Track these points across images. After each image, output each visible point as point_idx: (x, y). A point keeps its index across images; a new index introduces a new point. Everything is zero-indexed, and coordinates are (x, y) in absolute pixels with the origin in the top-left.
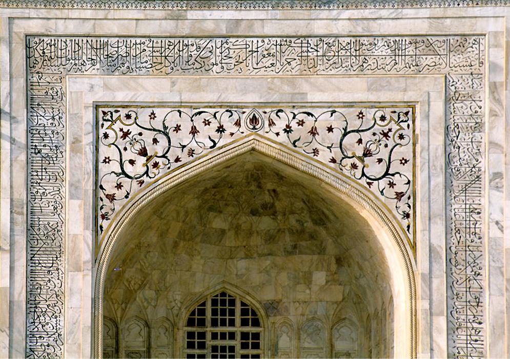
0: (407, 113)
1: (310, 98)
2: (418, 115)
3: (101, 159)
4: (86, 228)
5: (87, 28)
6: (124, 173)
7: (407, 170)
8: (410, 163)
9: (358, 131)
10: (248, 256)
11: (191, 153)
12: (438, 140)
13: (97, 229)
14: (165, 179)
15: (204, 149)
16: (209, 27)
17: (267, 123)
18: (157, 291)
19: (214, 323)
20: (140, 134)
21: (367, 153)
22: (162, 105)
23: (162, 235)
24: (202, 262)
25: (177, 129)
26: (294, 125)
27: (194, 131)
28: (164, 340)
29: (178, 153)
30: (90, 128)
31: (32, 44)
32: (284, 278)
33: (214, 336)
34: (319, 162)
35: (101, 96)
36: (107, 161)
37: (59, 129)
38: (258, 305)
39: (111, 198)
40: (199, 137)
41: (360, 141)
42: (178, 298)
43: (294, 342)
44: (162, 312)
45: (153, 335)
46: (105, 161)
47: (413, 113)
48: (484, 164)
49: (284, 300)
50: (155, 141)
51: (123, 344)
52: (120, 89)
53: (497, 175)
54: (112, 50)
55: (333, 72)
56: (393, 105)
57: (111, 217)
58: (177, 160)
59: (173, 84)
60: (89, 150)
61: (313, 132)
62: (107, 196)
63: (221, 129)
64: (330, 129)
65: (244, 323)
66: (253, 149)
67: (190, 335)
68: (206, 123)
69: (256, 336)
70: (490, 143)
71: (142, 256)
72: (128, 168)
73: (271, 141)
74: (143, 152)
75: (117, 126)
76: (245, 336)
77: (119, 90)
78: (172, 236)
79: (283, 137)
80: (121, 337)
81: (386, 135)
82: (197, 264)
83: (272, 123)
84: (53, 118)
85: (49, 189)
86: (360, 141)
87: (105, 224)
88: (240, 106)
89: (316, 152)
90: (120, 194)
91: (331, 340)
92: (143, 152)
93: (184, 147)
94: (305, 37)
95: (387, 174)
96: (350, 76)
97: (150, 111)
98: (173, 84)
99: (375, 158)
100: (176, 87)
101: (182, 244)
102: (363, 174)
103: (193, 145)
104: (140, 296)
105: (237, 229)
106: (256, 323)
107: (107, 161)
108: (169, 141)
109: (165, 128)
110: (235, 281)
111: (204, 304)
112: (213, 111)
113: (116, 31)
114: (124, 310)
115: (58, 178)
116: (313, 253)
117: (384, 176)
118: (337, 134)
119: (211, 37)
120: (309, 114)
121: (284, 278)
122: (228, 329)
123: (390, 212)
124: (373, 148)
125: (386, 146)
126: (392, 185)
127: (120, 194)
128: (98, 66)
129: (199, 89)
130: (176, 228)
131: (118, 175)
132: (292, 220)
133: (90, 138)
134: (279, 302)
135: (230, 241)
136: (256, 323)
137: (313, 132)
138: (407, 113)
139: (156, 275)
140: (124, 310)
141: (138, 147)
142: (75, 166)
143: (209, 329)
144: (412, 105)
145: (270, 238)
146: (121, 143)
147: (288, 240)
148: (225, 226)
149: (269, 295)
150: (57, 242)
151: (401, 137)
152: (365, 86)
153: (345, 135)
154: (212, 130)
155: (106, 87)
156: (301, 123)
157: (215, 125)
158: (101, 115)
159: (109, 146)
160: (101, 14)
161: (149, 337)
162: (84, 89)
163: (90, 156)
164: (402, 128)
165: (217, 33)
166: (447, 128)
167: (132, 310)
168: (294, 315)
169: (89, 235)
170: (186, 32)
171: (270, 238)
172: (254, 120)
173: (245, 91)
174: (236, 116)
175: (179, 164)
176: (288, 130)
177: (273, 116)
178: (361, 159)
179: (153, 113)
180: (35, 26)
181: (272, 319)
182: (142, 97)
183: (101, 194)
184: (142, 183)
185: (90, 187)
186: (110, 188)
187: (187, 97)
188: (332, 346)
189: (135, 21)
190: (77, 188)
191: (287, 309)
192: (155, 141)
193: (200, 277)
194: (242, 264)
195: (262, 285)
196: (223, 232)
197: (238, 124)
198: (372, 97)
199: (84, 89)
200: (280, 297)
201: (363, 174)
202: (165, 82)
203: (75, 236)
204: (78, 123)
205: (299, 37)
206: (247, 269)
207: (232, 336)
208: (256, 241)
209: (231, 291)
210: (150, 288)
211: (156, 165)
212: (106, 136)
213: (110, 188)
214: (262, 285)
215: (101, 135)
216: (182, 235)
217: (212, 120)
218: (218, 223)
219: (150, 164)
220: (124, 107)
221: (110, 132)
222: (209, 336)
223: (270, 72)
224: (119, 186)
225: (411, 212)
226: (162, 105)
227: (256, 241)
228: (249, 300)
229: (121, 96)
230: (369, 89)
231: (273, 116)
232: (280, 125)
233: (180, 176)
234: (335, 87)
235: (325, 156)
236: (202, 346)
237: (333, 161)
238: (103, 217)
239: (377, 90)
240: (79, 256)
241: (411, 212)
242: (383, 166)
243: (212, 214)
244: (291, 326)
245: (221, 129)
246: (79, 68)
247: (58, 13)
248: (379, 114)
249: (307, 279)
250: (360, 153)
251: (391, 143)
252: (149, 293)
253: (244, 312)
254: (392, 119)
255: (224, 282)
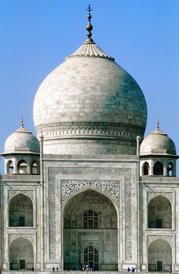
0: (118, 182)
1: (100, 179)
2: (120, 183)
3: (62, 190)
4: (60, 203)
5: (59, 166)
6: (66, 193)
7: (118, 193)
8: (119, 191)
9: (109, 185)
10: (95, 203)
11: (79, 189)
12: (124, 187)
13: (61, 203)
14: (74, 194)
15: (82, 188)
16: (82, 166)
17: (93, 184)
18: (78, 210)
19: (89, 216)
20: (69, 185)
21: (111, 189)
22: (73, 180)
23: (77, 200)
24: (86, 204)
25: (76, 184)
26: (97, 184)
27: (79, 185)
28: (79, 219)
29: (76, 189)
30: (60, 184)
31: (49, 169)
32: (102, 207)
33: (89, 218)
34: (102, 191)
35: (62, 178)
36: (63, 190)
37: (55, 184)
38: (97, 212)
39: (64, 197)
40: (80, 186)
41: (110, 187)
42: (82, 211)
43: (104, 219)
44: (79, 214)
45: (77, 218)
46: (63, 190)
47: (119, 182)
48: (132, 192)
49: (102, 212)
50: (72, 187)
51: (71, 219)
52: (65, 177)
53: (134, 194)
54: (64, 170)
55: (105, 174)
56: (116, 181)
57: (64, 201)
58: (76, 190)
59: (75, 176)
60: (60, 188)
61: (101, 185)
62: (63, 197)
63: (84, 185)
64: (104, 185)
65: (95, 216)
66: (90, 188)
67: (84, 218)
68: (82, 183)
69: (97, 218)
70: (133, 188)
71: (74, 203)
72: (67, 192)
73: (93, 187)
74: (70, 189)
75: (65, 184)
76: (95, 218)
77: (66, 177)
78: (79, 200)
79: (95, 186)
80: (71, 218)
81: (114, 186)
82: (85, 205)
83: (93, 184)
84: (53, 182)
85: (53, 195)
86: (110, 187)
87: (63, 202)
88: (88, 181)
89: (101, 189)
90: (66, 196)
91: (111, 219)
92: (70, 189)
93: (77, 188)
94: (99, 168)
95: (114, 193)
96: (108, 175)
97: (71, 181)
98: (75, 176)
99: (112, 190)
100: (76, 177)
101: (81, 201)
102: (110, 193)
103: (79, 188)
104: (74, 211)
105: (92, 199)
106: (97, 216)
107: (63, 190)
108: (75, 187)
109: (74, 184)
110: (92, 207)
111: (87, 212)
112: (83, 181)
113: (65, 167)
114: (71, 213)
115: (54, 193)
116: (107, 203)
117: (114, 194)
118: (105, 186)
119: (82, 168)
120: (100, 182)
121: (102, 207)
122: (91, 217)
123: (115, 200)
124: (112, 188)
125: (114, 188)
126: (115, 195)
127: (66, 196)
128: (61, 173)
129: (80, 177)
130: (80, 199)
131: (65, 193)
132: (102, 198)
133: (60, 186)
134: (101, 212)
135: (91, 201)
136: (97, 216)
137: (101, 185)
138: (118, 182)
139: (77, 207)
140: (71, 213)
141: (69, 188)
142: (57, 191)
143: (88, 217)
144: (119, 181)
145: (98, 200)
146: (66, 187)
147: (102, 201)
148: (90, 198)
149: (99, 210)
150: (54, 205)
151: (117, 187)
152: (110, 177)
153: (107, 186)
154: (82, 185)
155: (63, 177)
156: (99, 184)
157: (83, 184)
158: (62, 182)
159: (64, 188)
160: (62, 163)
161: (76, 218)
162: (59, 177)
163: (60, 189)
164: (117, 185)
165: (83, 167)
166: (125, 185)
167: (73, 213)
168: (104, 214)
169: (60, 204)
170: (77, 167)
171: (98, 200)
172: (90, 183)
173: (89, 178)
174: (87, 182)
175: (76, 191)
176: (96, 185)
177: (94, 182)
178: (110, 191)
179: (72, 182)
180: (50, 166)
181: (100, 215)
182: (70, 179)
183: (62, 196)
184: (70, 194)
185: (60, 195)
186: (64, 195)
187: (78, 179)
188: (111, 220)
189: (68, 165)
190: (58, 196)
191: (103, 213)
192: (72, 187)
193: (86, 207)
194: (94, 205)
195: (98, 209)
196: (89, 199)
197: (87, 184)
198: (112, 179)
199: (59, 177)
200: (101, 211)
201: (110, 193)
202: (74, 176)
203: (58, 204)
204: (57, 183)
205: (98, 168)
206: (95, 206)
207: (92, 218)
208: (96, 201)
209: (92, 209)
210: (76, 209)
211: (72, 191)
212: (63, 186)
213: (64, 196)
214: (98, 209)
215: (62, 186)
216: (81, 200)
217: (83, 183)
218: (88, 198)
219: (71, 191)
220: (66, 180)
221: (64, 185)
222: (88, 218)
223: (93, 174)
224: (66, 195)
225: (119, 200)
226: (73, 180)
227: (96, 201)
228: (95, 211)
229: (66, 179)
230: (111, 178)
231: (94, 182)
232: (95, 184)
233: (77, 193)
234: (105, 177)
235: (103, 190)
236: (87, 220)
237: (105, 191)
238: (63, 201)
239: (112, 178)
240: (58, 208)
241: (119, 200)
242: (114, 192)
243: (87, 196)
244: (103, 216)
245: (84, 185)
246: (58, 173)
247: (54, 163)
248: (113, 182)
249: (106, 208)
250: (110, 190)
251: (115, 188)
252: (76, 210)
253: (94, 213)
254: (115, 183)
255: (90, 208)
